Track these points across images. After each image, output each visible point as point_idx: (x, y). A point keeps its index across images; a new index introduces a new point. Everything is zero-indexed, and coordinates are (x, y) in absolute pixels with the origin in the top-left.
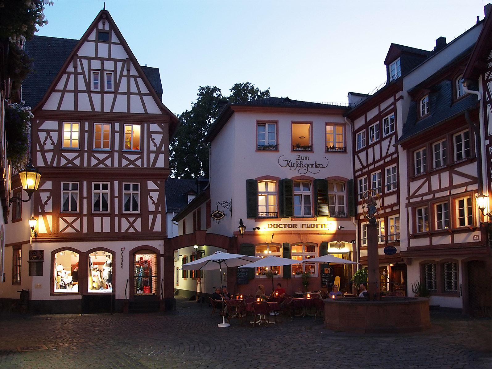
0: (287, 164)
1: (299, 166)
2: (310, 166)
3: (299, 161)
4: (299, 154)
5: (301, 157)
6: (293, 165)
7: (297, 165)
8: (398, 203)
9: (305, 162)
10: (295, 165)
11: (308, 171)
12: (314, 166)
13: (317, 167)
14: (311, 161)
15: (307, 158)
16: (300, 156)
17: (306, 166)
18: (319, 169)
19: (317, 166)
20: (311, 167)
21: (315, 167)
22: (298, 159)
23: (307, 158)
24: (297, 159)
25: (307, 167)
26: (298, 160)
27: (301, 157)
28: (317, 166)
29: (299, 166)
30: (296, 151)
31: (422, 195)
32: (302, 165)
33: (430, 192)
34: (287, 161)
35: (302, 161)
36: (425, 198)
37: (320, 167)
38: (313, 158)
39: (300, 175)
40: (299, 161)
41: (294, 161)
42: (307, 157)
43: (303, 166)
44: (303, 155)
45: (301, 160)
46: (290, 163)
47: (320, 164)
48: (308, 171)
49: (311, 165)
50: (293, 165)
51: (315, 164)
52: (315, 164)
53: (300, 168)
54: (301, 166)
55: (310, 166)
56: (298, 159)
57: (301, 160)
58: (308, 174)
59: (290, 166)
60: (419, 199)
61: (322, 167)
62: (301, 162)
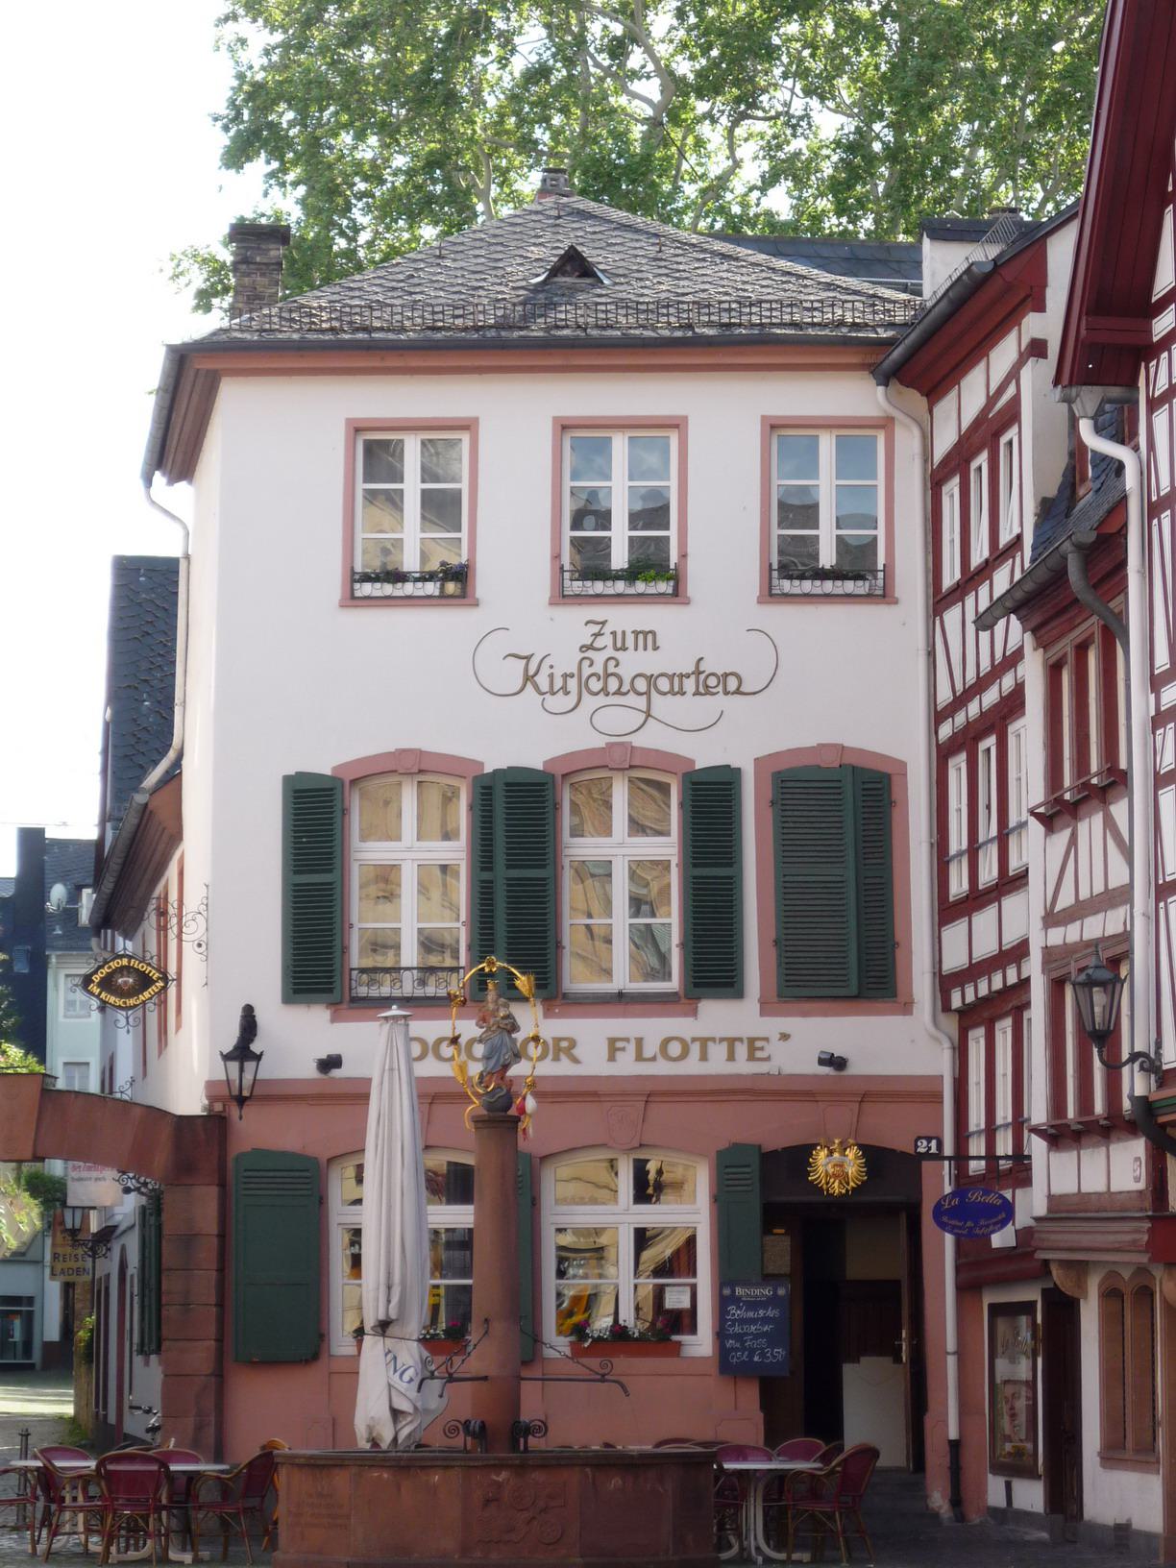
0: (529, 678)
1: (595, 685)
2: (664, 684)
3: (599, 658)
4: (598, 612)
5: (614, 633)
6: (558, 683)
7: (583, 685)
9: (633, 663)
10: (573, 684)
11: (648, 715)
12: (690, 685)
13: (708, 691)
14: (672, 658)
15: (647, 638)
16: (607, 630)
17: (641, 685)
18: (719, 701)
19: (706, 682)
20: (672, 692)
21: (697, 693)
22: (590, 647)
23: (647, 638)
24: (585, 648)
25: (648, 693)
26: (590, 654)
27: (614, 633)
28: (706, 682)
29: (595, 685)
30: (580, 599)
32: (613, 684)
34: (528, 658)
35: (619, 655)
37: (726, 693)
38: (679, 634)
39: (600, 742)
40: (599, 658)
41: (566, 660)
42: (646, 634)
43: (624, 689)
44: (625, 618)
45: (610, 652)
46: (545, 671)
47: (726, 675)
48: (648, 715)
49: (671, 677)
50: (558, 683)
51: (698, 672)
52: (698, 672)
53: (601, 700)
54: (610, 684)
55: (664, 684)
56: (590, 647)
57: (610, 652)
58: (653, 738)
59: (544, 686)
61: (738, 692)
62: (612, 663)
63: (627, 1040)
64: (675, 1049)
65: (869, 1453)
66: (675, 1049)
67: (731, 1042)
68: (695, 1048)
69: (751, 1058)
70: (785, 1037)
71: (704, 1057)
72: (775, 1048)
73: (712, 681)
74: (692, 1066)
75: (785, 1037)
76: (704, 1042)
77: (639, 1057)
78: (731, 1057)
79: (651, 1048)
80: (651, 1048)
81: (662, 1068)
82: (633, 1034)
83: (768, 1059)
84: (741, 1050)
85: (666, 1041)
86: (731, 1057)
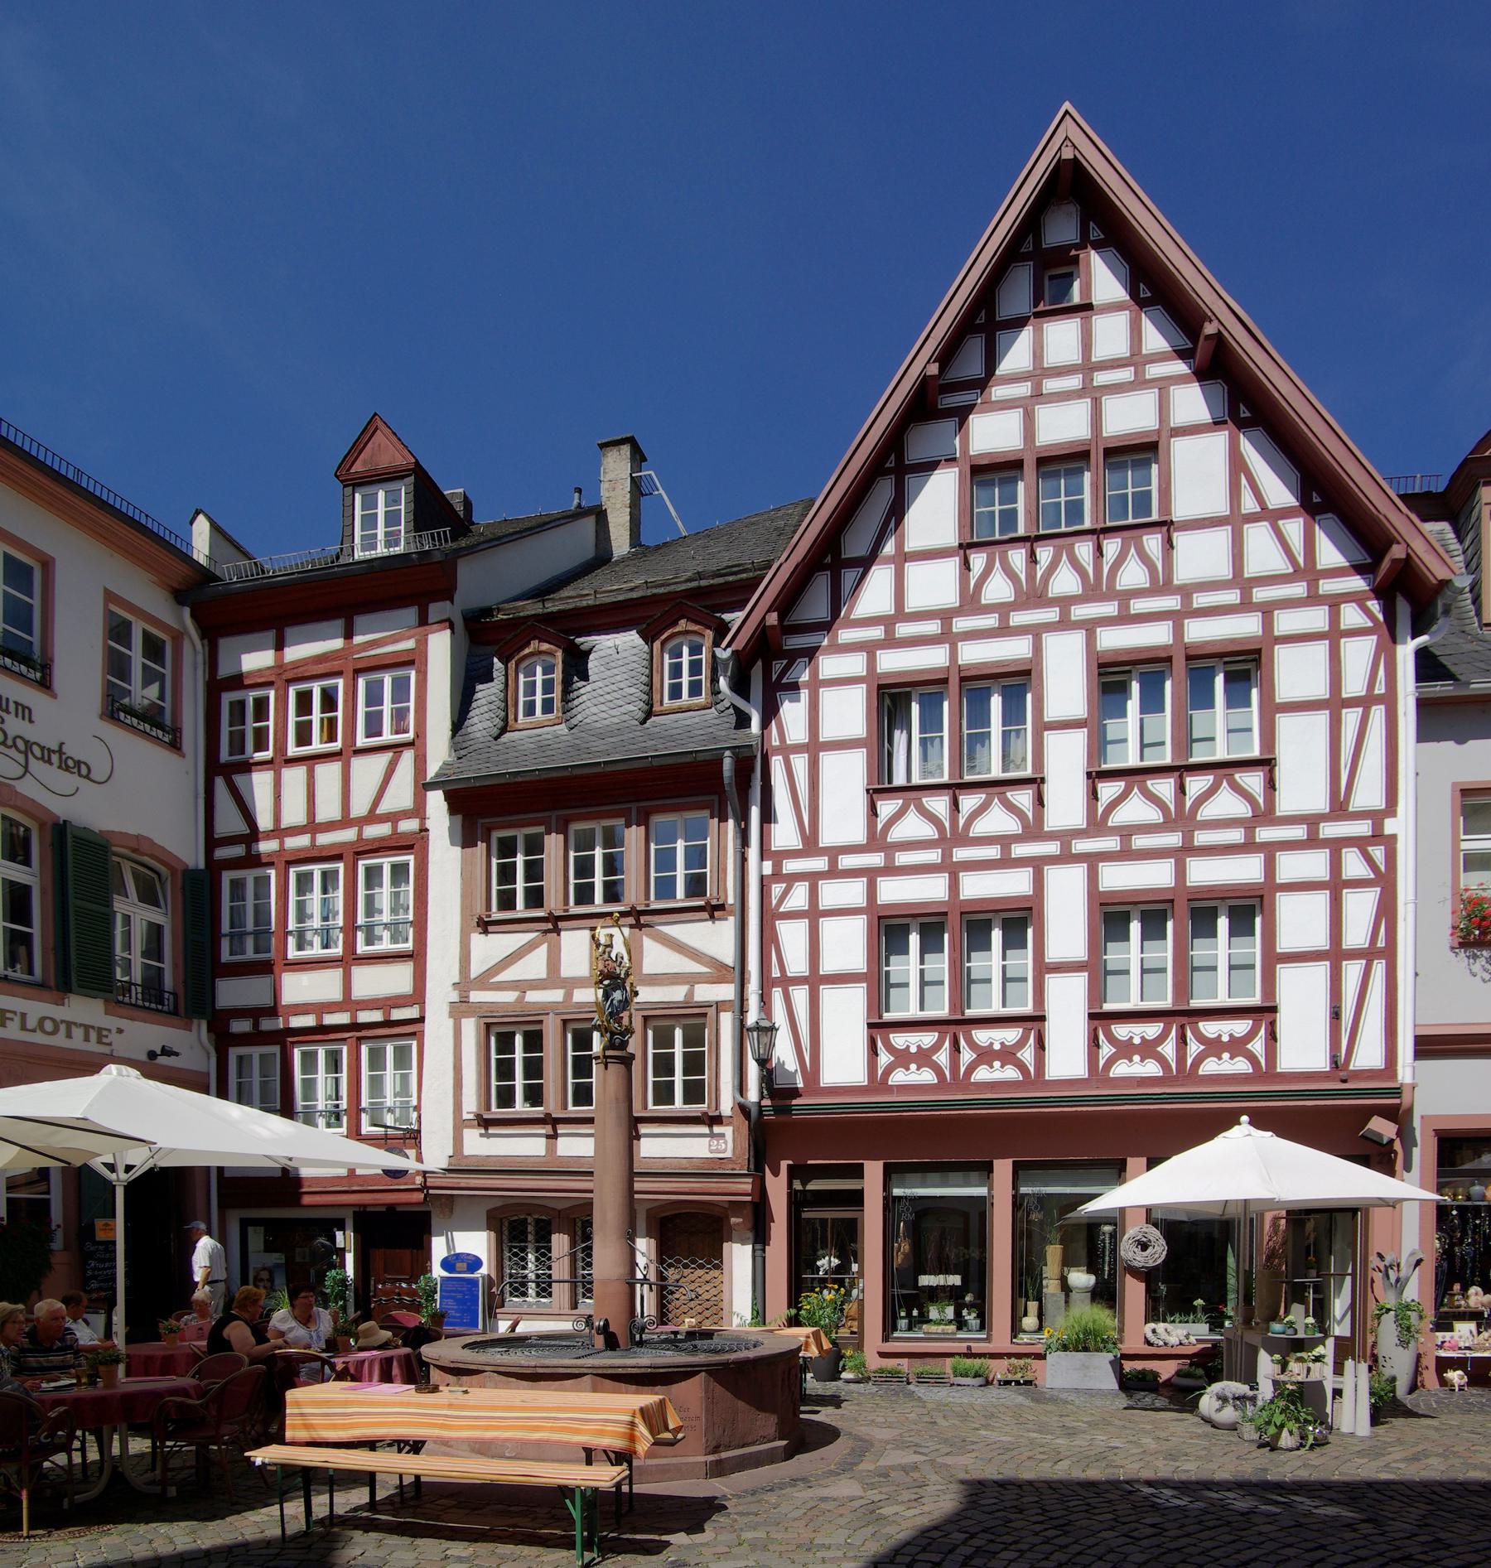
8: (418, 996)
13: (67, 769)
31: (522, 986)
33: (553, 978)
36: (533, 996)
52: (60, 752)
60: (509, 997)
61: (87, 777)
63: (15, 1013)
64: (49, 1026)
65: (75, 1321)
66: (49, 1026)
67: (87, 1028)
68: (63, 1027)
69: (99, 1042)
70: (120, 1031)
71: (69, 1036)
72: (113, 1037)
73: (71, 763)
74: (59, 1040)
75: (120, 1031)
76: (69, 1024)
77: (24, 1027)
78: (87, 1039)
79: (32, 1023)
80: (32, 1023)
81: (39, 1038)
82: (20, 1010)
83: (110, 1044)
84: (93, 1035)
85: (42, 1020)
86: (87, 1039)
